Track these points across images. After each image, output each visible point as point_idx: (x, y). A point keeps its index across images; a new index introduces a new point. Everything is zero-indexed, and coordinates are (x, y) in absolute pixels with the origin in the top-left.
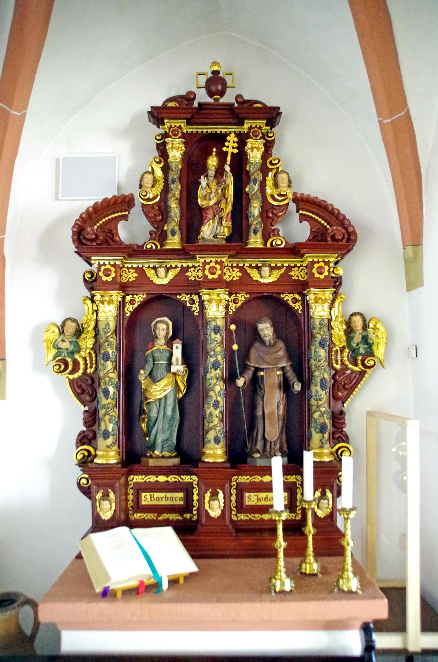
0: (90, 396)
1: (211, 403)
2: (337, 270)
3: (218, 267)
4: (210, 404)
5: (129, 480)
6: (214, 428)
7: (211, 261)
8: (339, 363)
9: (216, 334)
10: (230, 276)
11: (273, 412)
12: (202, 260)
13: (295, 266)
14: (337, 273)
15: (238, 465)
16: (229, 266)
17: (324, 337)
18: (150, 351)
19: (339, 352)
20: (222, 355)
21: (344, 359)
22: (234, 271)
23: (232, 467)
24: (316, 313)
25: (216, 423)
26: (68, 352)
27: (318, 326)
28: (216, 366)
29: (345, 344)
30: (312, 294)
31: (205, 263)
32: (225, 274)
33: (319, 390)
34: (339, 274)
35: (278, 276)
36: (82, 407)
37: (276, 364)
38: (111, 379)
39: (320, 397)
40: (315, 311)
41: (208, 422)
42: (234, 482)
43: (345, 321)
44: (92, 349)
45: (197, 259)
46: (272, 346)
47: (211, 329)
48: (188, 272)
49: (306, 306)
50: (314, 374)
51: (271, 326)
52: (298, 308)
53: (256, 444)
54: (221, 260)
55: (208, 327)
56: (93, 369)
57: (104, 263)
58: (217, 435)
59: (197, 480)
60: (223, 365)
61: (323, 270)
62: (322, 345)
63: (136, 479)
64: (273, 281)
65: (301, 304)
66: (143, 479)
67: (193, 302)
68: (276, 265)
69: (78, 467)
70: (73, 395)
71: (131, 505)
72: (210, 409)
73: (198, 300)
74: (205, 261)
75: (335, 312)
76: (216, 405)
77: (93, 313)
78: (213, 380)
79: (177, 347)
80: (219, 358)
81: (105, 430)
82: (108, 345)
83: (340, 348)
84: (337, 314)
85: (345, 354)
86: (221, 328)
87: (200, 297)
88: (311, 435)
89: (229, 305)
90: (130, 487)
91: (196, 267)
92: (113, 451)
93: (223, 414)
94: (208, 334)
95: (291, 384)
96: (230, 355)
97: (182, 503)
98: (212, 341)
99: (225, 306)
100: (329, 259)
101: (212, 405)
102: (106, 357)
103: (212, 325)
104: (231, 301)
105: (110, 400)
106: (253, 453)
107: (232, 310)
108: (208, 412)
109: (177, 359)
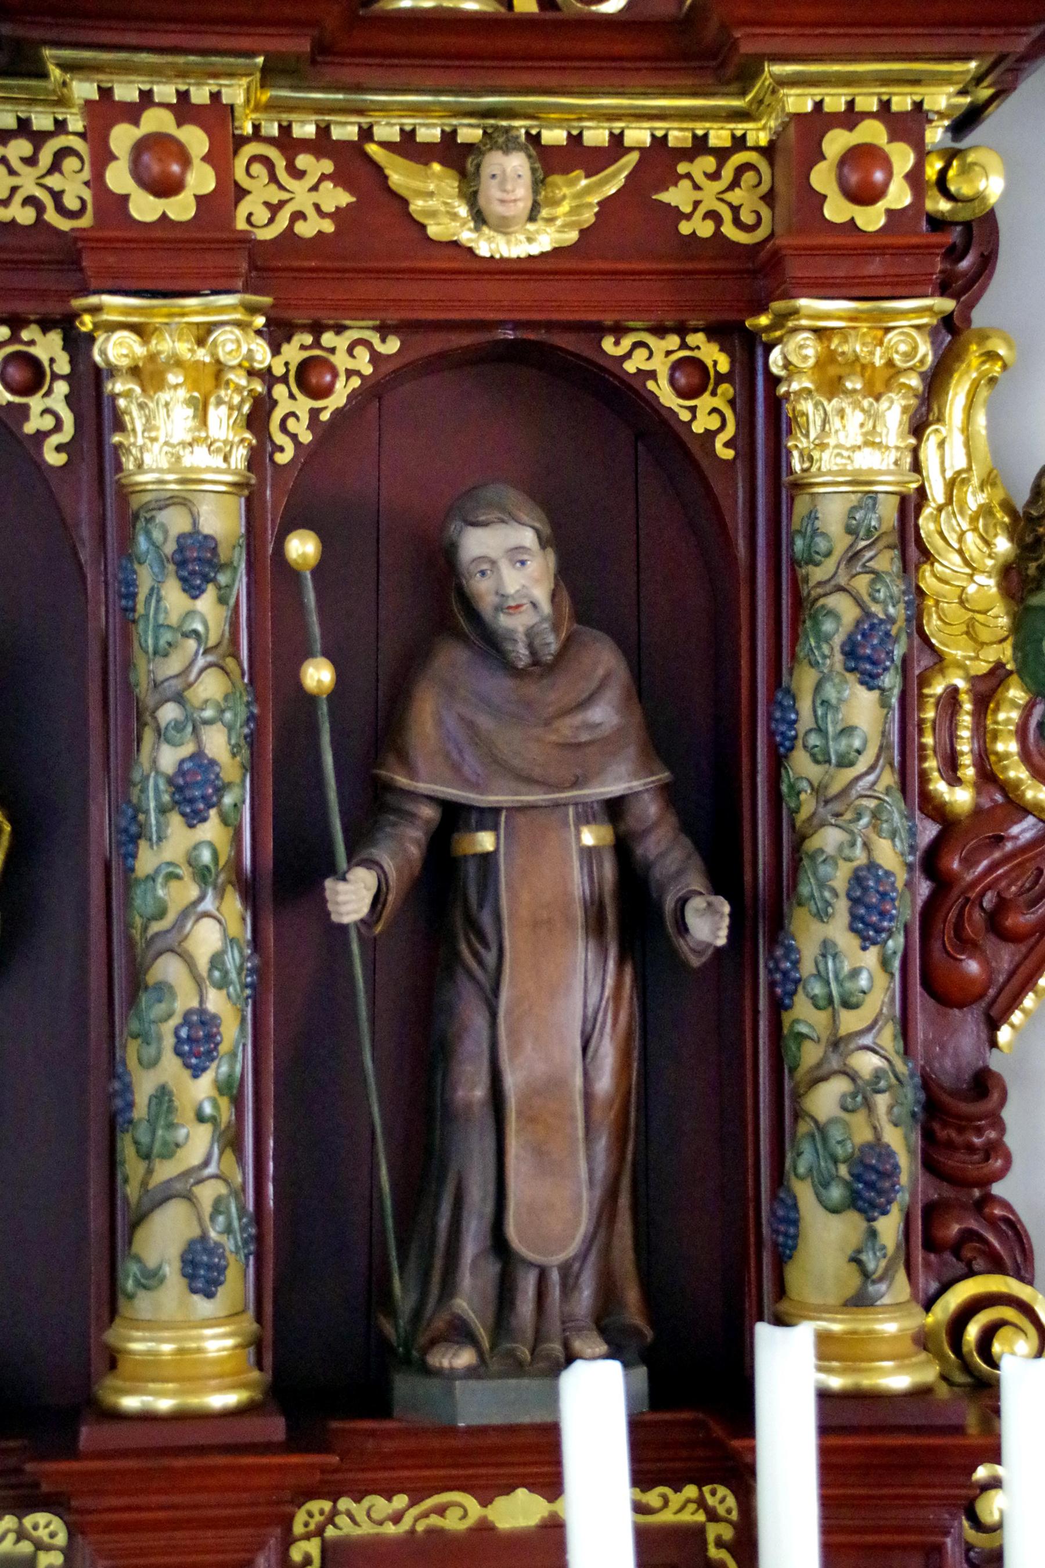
1: (168, 1028)
2: (966, 170)
3: (195, 140)
4: (160, 1038)
6: (180, 1190)
7: (146, 97)
8: (969, 772)
9: (194, 591)
10: (274, 209)
11: (556, 1084)
12: (84, 90)
13: (700, 146)
14: (966, 190)
15: (335, 1425)
16: (270, 141)
17: (875, 608)
19: (968, 706)
20: (230, 728)
21: (1000, 747)
22: (298, 174)
23: (294, 1443)
24: (827, 461)
25: (196, 1160)
27: (841, 543)
28: (193, 794)
29: (1006, 653)
30: (801, 337)
31: (105, 112)
32: (242, 193)
33: (846, 941)
34: (980, 197)
35: (588, 217)
37: (575, 784)
39: (847, 984)
40: (822, 446)
41: (146, 1156)
42: (307, 1537)
43: (1008, 507)
45: (44, 75)
46: (542, 668)
47: (162, 561)
49: (765, 415)
50: (813, 843)
51: (543, 543)
52: (714, 423)
53: (449, 1287)
54: (215, 96)
55: (142, 543)
58: (204, 1237)
60: (238, 796)
61: (879, 176)
62: (861, 659)
64: (557, 252)
65: (732, 403)
67: (33, 376)
68: (575, 140)
72: (156, 1072)
73: (63, 366)
74: (106, 93)
75: (946, 453)
76: (198, 1043)
78: (174, 884)
80: (217, 744)
83: (974, 680)
84: (957, 459)
85: (1002, 716)
86: (224, 555)
87: (77, 345)
88: (795, 1223)
89: (275, 403)
93: (237, 1102)
94: (143, 592)
95: (669, 904)
96: (281, 729)
98: (167, 636)
99: (246, 408)
100: (918, 93)
101: (169, 1041)
104: (284, 379)
106: (433, 1342)
107: (294, 437)
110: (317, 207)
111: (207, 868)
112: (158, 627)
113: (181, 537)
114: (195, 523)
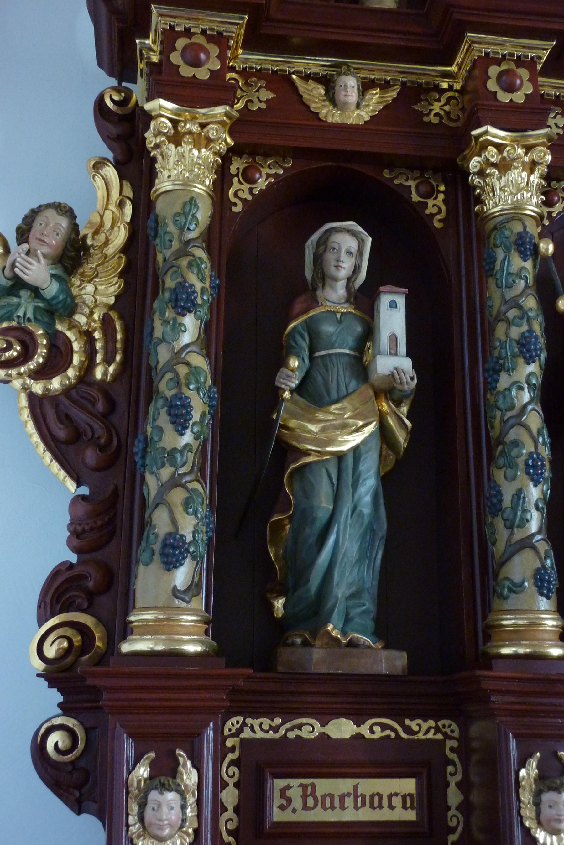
0: (102, 449)
4: (517, 466)
5: (226, 732)
18: (304, 317)
26: (36, 309)
36: (71, 485)
38: (194, 371)
41: (510, 526)
44: (112, 307)
48: (418, 100)
56: (111, 369)
57: (187, 30)
58: (544, 567)
59: (456, 734)
63: (252, 728)
66: (276, 729)
69: (43, 683)
70: (42, 447)
71: (231, 826)
76: (533, 472)
77: (121, 205)
78: (521, 392)
79: (393, 305)
81: (169, 534)
82: (190, 265)
90: (231, 756)
91: (445, 91)
92: (193, 612)
97: (411, 815)
101: (522, 466)
102: (183, 302)
103: (512, 232)
105: (187, 438)
108: (508, 494)
109: (393, 339)
110: (556, 124)
111: (534, 385)
112: (509, 274)
113: (519, 233)
114: (525, 227)
